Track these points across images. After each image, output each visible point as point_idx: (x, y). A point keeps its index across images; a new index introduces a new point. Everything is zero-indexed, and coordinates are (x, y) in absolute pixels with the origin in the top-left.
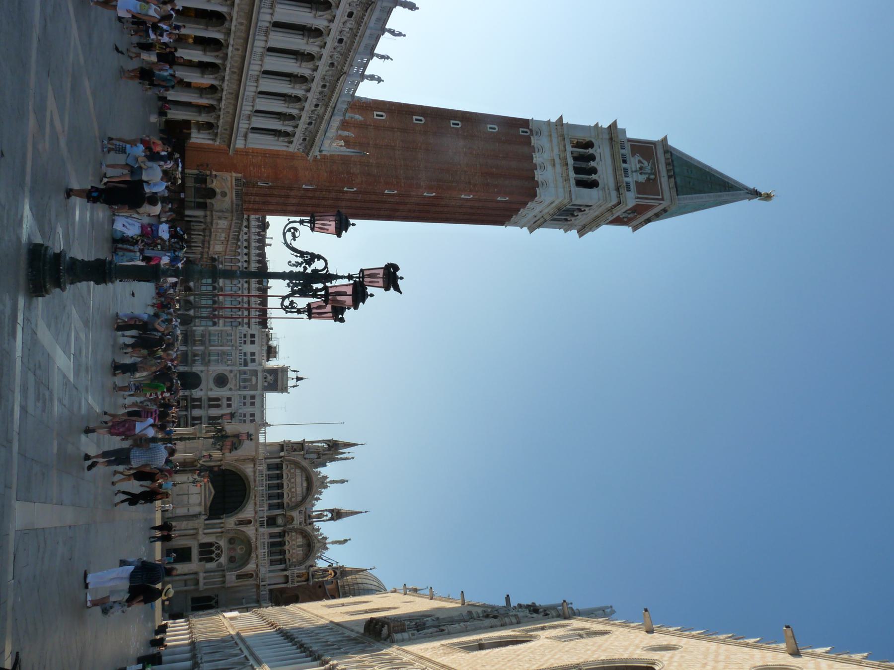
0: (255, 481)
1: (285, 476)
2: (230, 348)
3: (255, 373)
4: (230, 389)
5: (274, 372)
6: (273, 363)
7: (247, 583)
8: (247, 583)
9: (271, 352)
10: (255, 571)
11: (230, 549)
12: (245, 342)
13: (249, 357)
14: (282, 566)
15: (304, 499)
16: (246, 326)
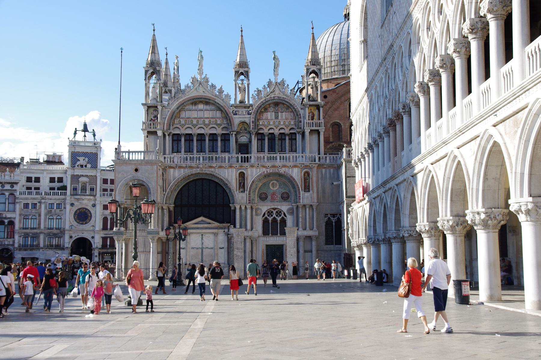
0: (191, 167)
1: (189, 131)
2: (43, 206)
3: (75, 178)
4: (94, 205)
5: (74, 157)
6: (66, 158)
7: (314, 179)
8: (314, 179)
9: (54, 160)
10: (302, 169)
11: (273, 200)
12: (38, 188)
13: (56, 185)
14: (299, 137)
15: (219, 108)
16: (16, 187)
